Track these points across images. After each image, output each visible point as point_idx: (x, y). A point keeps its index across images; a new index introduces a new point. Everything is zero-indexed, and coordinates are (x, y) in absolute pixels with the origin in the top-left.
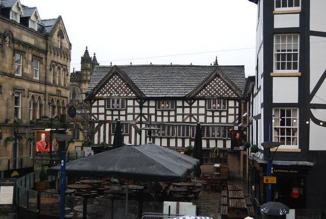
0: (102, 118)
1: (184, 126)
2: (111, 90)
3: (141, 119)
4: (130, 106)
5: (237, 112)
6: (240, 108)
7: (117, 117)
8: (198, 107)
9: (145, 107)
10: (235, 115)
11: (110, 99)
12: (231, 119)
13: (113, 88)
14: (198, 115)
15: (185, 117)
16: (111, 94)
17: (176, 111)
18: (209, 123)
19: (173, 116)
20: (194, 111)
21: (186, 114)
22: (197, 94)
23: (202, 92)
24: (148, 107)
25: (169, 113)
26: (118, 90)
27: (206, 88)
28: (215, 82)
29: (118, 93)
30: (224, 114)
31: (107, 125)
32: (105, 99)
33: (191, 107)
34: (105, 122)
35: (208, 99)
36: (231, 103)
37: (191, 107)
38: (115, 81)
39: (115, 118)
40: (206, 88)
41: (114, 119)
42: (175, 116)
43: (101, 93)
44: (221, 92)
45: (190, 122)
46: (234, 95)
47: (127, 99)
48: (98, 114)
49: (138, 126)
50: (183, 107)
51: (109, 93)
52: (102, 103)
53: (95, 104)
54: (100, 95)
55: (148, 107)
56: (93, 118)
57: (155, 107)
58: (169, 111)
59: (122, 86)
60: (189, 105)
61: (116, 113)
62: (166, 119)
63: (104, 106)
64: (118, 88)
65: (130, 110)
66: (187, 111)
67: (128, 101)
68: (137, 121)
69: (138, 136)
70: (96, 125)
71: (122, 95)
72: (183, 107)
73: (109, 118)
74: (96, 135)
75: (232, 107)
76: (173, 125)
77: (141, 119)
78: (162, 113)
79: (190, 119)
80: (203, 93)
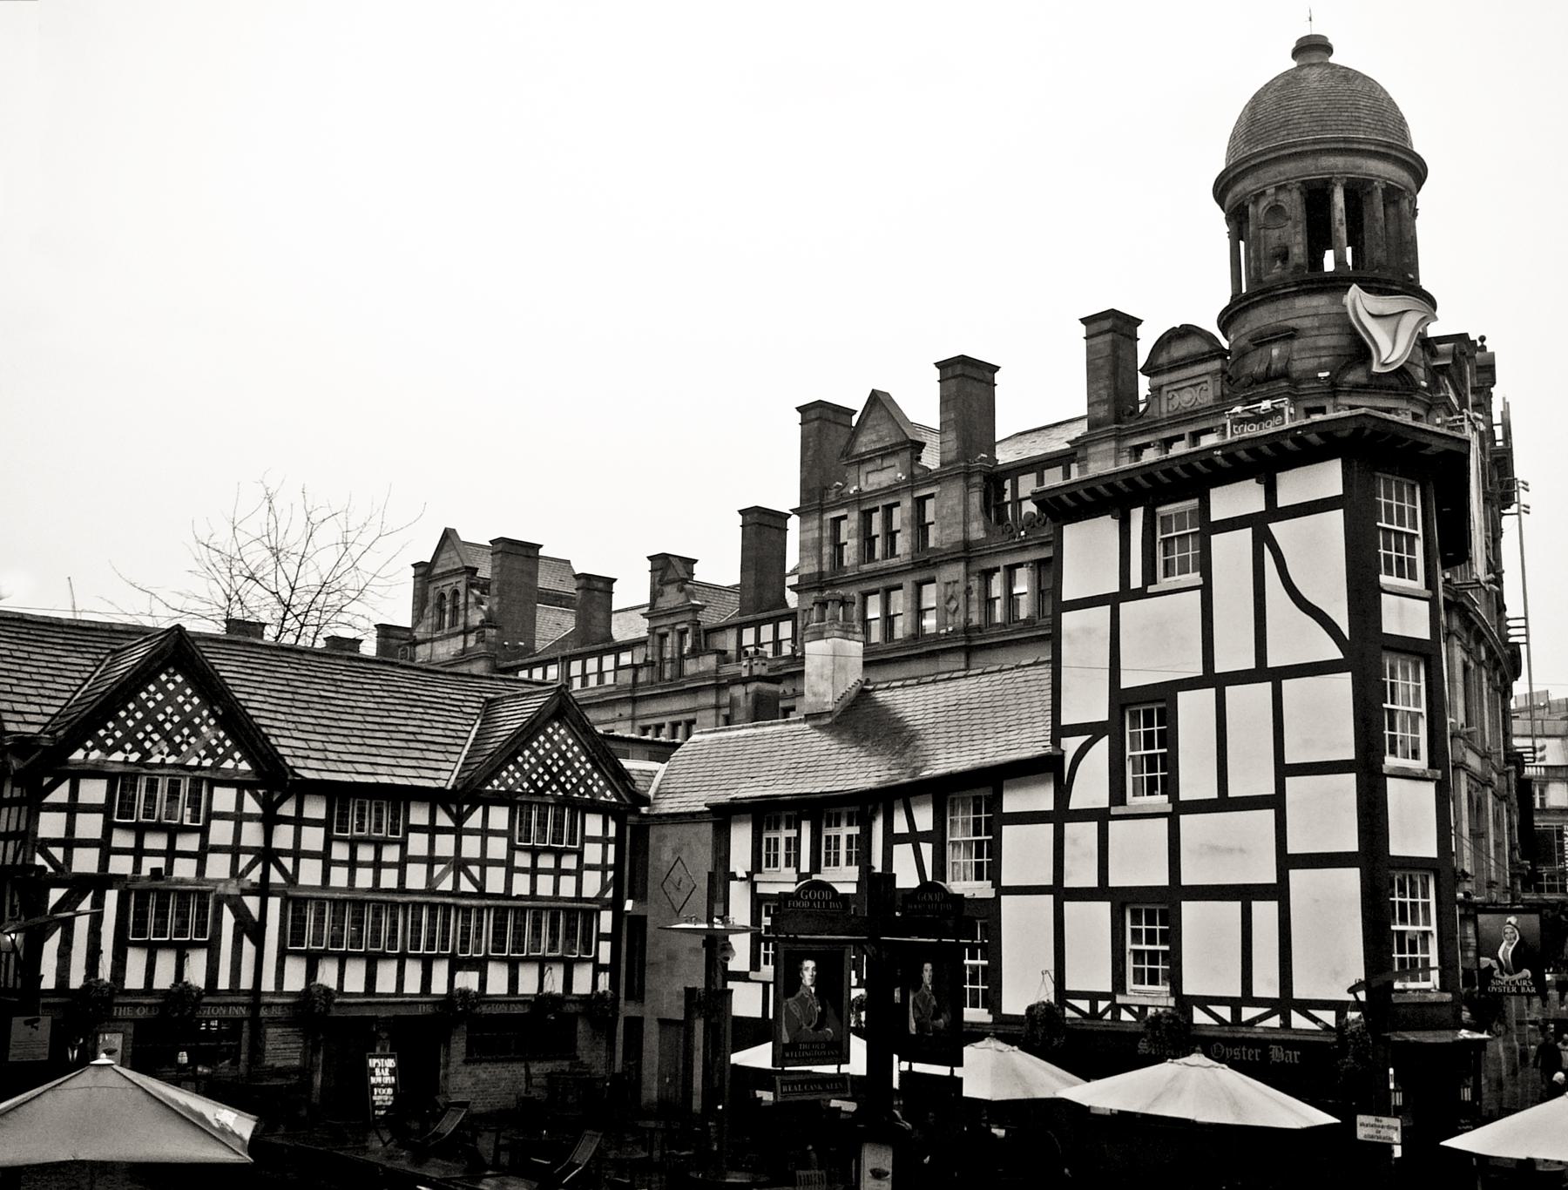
0: (85, 861)
1: (433, 907)
2: (148, 736)
3: (265, 875)
4: (223, 816)
5: (611, 860)
6: (619, 841)
7: (160, 862)
8: (485, 832)
9: (285, 820)
10: (603, 867)
11: (135, 776)
12: (592, 884)
13: (158, 727)
14: (484, 862)
15: (438, 869)
16: (147, 754)
17: (404, 844)
18: (519, 897)
19: (390, 865)
20: (471, 847)
21: (442, 860)
22: (488, 781)
23: (504, 774)
24: (299, 822)
25: (378, 853)
26: (178, 739)
27: (520, 759)
28: (549, 738)
29: (175, 750)
30: (569, 862)
31: (111, 897)
32: (112, 778)
33: (458, 832)
34: (100, 882)
35: (523, 803)
36: (594, 825)
37: (458, 832)
38: (170, 698)
39: (149, 864)
40: (520, 759)
41: (145, 872)
42: (401, 866)
43: (100, 745)
44: (569, 780)
45: (456, 893)
46: (608, 793)
47: (213, 783)
48: (70, 842)
49: (252, 903)
50: (432, 830)
51: (138, 745)
52: (93, 791)
53: (61, 794)
54: (95, 755)
55: (299, 822)
56: (39, 860)
57: (325, 824)
58: (379, 845)
59: (197, 721)
60: (451, 824)
61: (156, 841)
62: (364, 878)
63: (105, 809)
64: (178, 729)
65: (221, 832)
66: (445, 845)
67: (217, 790)
68: (246, 885)
69: (248, 948)
70: (56, 895)
71: (194, 762)
72: (432, 830)
73: (121, 865)
74: (51, 946)
75: (594, 840)
76: (395, 905)
77: (265, 875)
78: (353, 852)
79: (456, 882)
80: (509, 779)
